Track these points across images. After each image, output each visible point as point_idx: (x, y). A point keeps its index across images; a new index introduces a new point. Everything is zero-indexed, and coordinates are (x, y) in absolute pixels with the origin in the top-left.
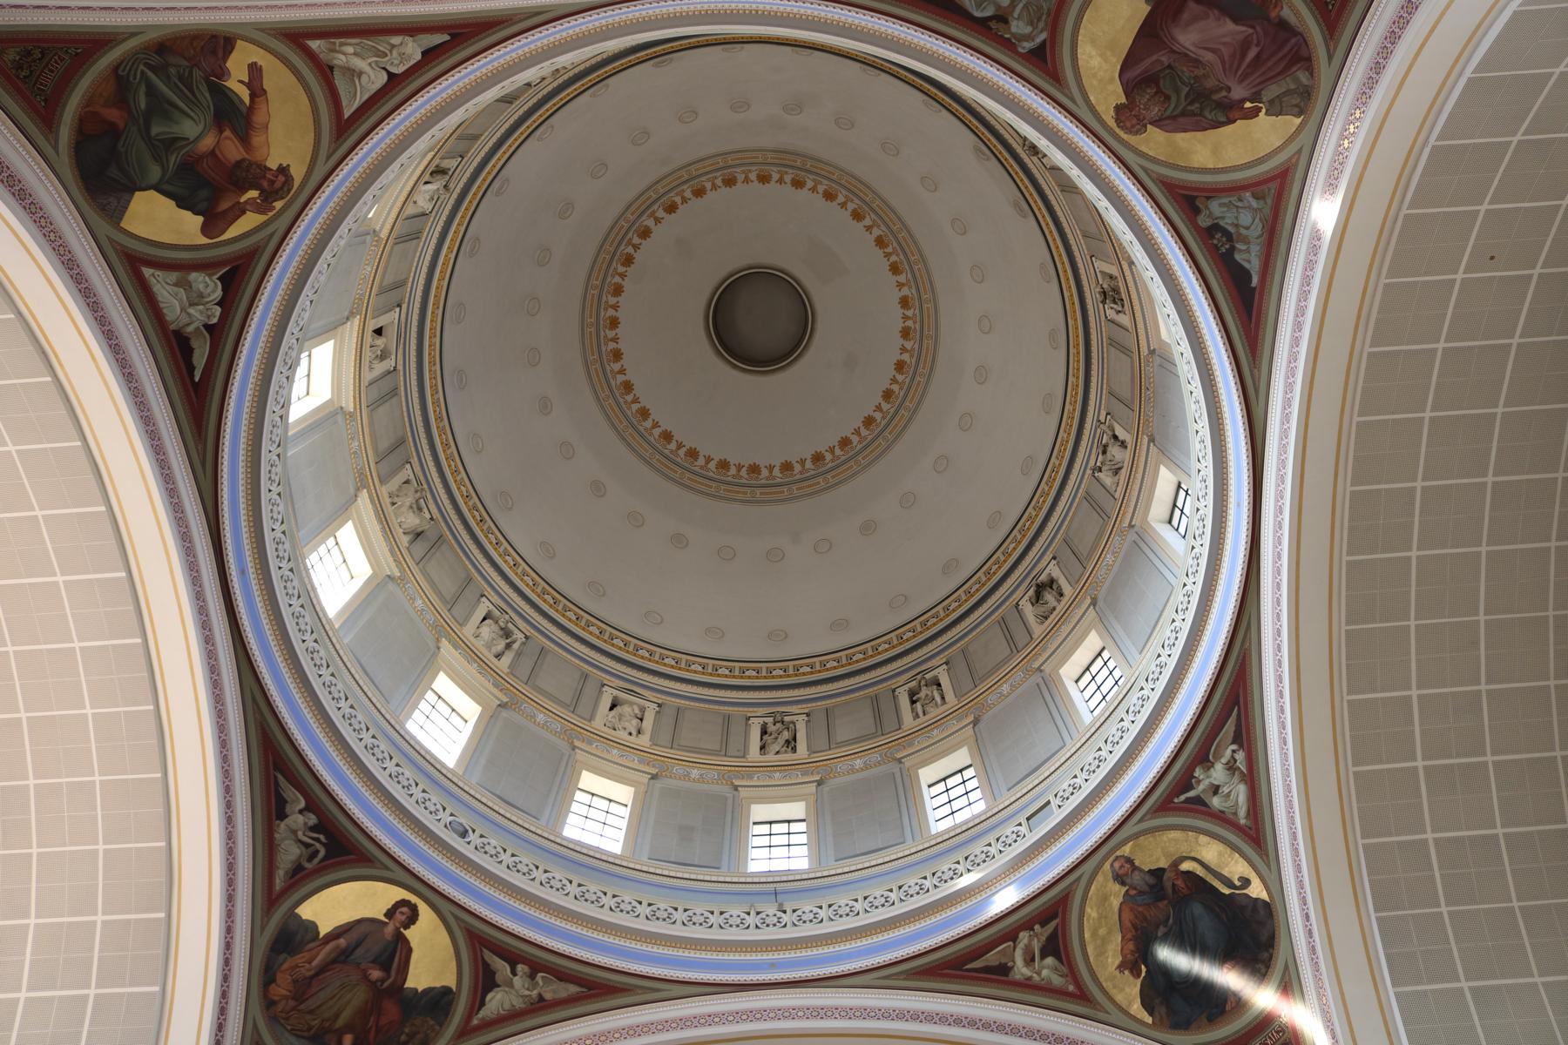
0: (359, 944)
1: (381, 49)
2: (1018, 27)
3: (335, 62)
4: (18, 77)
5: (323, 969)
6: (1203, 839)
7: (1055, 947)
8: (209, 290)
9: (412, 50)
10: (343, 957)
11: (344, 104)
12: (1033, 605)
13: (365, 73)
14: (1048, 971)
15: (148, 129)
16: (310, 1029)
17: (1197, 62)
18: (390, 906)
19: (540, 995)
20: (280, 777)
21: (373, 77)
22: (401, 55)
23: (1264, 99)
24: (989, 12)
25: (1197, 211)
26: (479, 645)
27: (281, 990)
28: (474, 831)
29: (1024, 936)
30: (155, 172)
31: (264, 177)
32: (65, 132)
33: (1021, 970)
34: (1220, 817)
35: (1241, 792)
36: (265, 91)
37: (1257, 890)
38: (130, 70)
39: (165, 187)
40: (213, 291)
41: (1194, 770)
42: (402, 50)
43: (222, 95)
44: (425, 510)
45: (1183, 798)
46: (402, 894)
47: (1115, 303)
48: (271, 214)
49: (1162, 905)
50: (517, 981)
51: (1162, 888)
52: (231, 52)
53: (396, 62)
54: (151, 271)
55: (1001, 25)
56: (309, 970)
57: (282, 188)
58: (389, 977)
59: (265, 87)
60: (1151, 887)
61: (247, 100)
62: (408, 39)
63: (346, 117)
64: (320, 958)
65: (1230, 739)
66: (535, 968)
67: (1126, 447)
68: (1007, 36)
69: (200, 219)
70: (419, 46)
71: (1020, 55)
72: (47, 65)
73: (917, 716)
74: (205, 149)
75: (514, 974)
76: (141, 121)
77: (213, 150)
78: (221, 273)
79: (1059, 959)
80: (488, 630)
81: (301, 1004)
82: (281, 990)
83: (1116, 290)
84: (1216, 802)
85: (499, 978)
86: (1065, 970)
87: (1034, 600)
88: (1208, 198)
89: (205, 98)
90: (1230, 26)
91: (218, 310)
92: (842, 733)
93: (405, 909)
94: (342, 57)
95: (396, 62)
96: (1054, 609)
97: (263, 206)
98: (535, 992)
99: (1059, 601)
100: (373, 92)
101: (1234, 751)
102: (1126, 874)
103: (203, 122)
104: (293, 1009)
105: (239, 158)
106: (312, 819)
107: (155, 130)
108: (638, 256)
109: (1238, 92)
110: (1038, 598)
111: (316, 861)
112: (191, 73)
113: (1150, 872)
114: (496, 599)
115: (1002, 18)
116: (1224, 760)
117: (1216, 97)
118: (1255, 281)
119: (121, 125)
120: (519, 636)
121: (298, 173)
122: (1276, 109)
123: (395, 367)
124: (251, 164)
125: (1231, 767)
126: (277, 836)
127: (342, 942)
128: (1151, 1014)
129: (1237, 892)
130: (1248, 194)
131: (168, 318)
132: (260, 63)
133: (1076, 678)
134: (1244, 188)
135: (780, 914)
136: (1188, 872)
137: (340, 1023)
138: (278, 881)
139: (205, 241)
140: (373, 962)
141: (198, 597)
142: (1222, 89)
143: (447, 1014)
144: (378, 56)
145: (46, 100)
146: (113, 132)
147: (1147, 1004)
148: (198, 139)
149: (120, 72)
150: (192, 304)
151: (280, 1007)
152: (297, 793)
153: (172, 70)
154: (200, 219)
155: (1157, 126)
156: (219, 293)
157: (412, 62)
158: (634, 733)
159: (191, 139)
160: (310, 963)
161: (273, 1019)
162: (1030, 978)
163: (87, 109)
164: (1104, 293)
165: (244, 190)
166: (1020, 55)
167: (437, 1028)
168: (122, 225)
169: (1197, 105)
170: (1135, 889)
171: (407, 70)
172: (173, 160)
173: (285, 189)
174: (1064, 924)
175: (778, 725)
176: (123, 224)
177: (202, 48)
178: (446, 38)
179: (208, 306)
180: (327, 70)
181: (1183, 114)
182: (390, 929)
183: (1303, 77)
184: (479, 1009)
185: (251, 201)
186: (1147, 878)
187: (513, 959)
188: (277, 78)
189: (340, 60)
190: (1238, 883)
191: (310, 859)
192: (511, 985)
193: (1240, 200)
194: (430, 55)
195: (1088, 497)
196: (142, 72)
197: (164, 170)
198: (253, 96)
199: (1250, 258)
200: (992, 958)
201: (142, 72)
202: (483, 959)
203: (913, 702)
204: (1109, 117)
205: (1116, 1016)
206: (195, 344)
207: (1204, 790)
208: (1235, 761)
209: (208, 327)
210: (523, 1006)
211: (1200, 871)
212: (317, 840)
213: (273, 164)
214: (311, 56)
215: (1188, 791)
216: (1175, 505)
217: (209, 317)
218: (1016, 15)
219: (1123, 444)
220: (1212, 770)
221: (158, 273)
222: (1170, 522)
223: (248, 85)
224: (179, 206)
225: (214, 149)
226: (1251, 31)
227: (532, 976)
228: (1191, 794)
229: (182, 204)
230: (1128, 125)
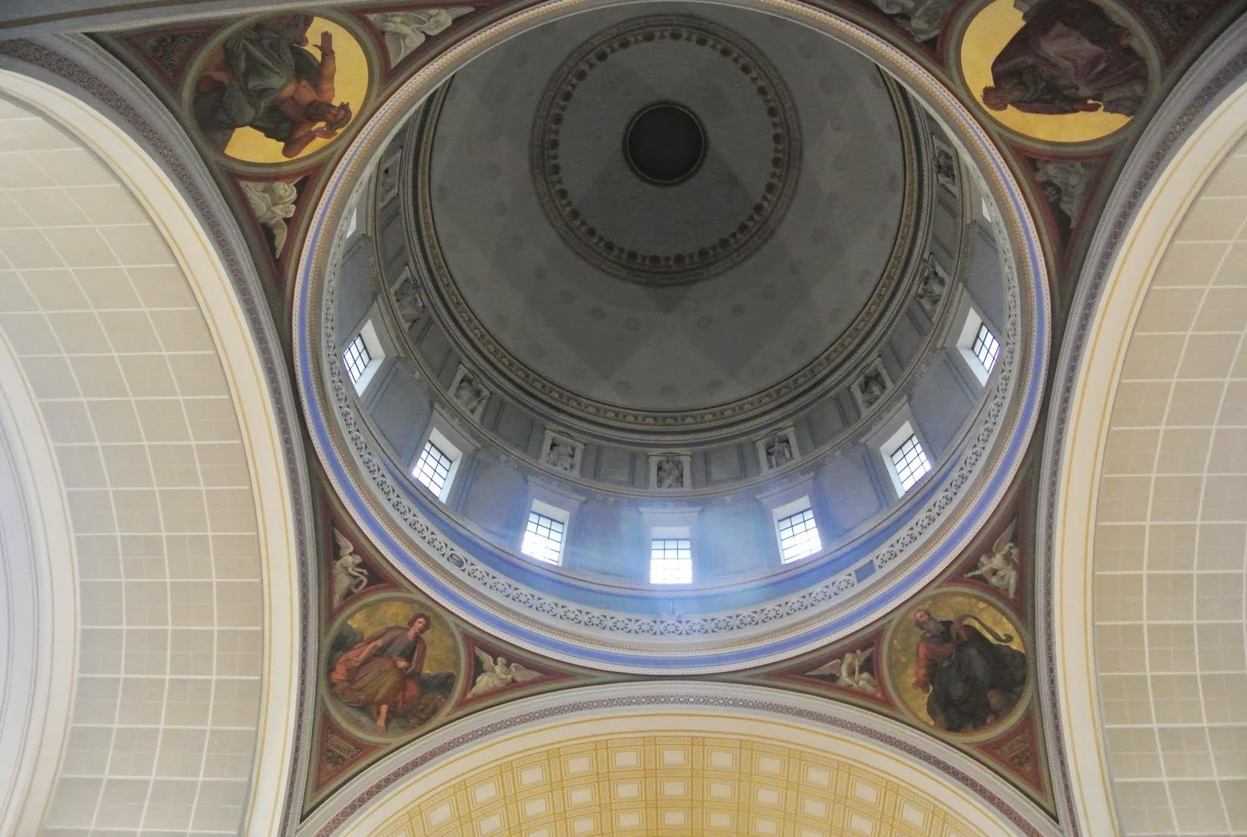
0: (390, 644)
1: (422, 18)
2: (917, 23)
3: (389, 29)
5: (366, 662)
6: (982, 605)
7: (869, 666)
8: (287, 194)
10: (380, 653)
11: (392, 58)
12: (862, 392)
14: (863, 681)
15: (246, 84)
16: (359, 701)
17: (1055, 66)
18: (411, 617)
19: (514, 681)
20: (336, 531)
22: (437, 22)
23: (1105, 99)
24: (896, 11)
25: (1036, 170)
26: (458, 402)
27: (339, 674)
28: (466, 561)
29: (849, 657)
30: (250, 113)
31: (330, 113)
32: (187, 92)
33: (845, 679)
34: (995, 591)
35: (1011, 577)
36: (332, 52)
37: (1016, 645)
39: (257, 123)
40: (290, 195)
41: (980, 557)
42: (438, 18)
44: (419, 300)
45: (970, 575)
46: (418, 610)
47: (948, 176)
48: (333, 138)
49: (949, 646)
50: (498, 668)
51: (949, 635)
54: (246, 183)
55: (904, 21)
56: (358, 662)
57: (344, 117)
58: (411, 666)
60: (943, 633)
61: (319, 58)
62: (443, 12)
64: (365, 653)
65: (1010, 536)
66: (510, 660)
67: (944, 285)
68: (907, 29)
69: (282, 144)
71: (916, 43)
73: (771, 467)
75: (496, 663)
77: (292, 97)
78: (296, 181)
79: (871, 672)
80: (466, 394)
81: (352, 684)
82: (339, 674)
83: (950, 168)
84: (994, 581)
85: (485, 666)
86: (876, 682)
87: (863, 388)
88: (1047, 162)
90: (1087, 45)
91: (293, 208)
92: (717, 473)
93: (421, 620)
96: (878, 398)
97: (326, 135)
98: (510, 676)
99: (882, 392)
101: (1011, 548)
102: (925, 622)
104: (348, 688)
105: (311, 99)
106: (358, 559)
107: (251, 85)
108: (576, 93)
109: (1084, 91)
110: (865, 387)
111: (361, 588)
113: (942, 622)
114: (469, 365)
115: (906, 16)
116: (1003, 553)
117: (1066, 92)
118: (1073, 225)
119: (227, 82)
120: (485, 393)
121: (355, 108)
122: (1112, 108)
123: (398, 194)
125: (1007, 558)
126: (334, 571)
127: (379, 643)
128: (934, 718)
129: (1003, 644)
130: (1078, 164)
131: (257, 216)
132: (330, 32)
133: (891, 453)
134: (1075, 158)
135: (678, 624)
136: (969, 628)
137: (379, 697)
138: (335, 602)
139: (285, 159)
140: (399, 656)
141: (280, 411)
142: (1072, 87)
143: (450, 691)
144: (419, 23)
146: (220, 87)
147: (931, 712)
148: (282, 89)
150: (274, 205)
151: (340, 686)
152: (349, 543)
153: (266, 42)
154: (282, 144)
155: (1018, 108)
156: (294, 196)
157: (445, 27)
158: (568, 467)
160: (358, 657)
161: (334, 696)
162: (850, 686)
164: (939, 167)
165: (314, 121)
166: (916, 43)
167: (444, 700)
168: (226, 152)
169: (1050, 96)
170: (929, 632)
171: (441, 32)
173: (345, 120)
174: (878, 652)
175: (671, 464)
176: (228, 152)
179: (287, 205)
181: (1038, 100)
182: (411, 634)
183: (1139, 89)
184: (472, 687)
185: (320, 129)
186: (940, 625)
187: (495, 654)
189: (390, 27)
190: (1004, 638)
191: (357, 586)
192: (493, 671)
193: (1072, 167)
194: (458, 22)
195: (909, 314)
198: (324, 56)
199: (1072, 208)
200: (825, 669)
201: (244, 45)
202: (474, 653)
203: (769, 454)
204: (978, 96)
205: (908, 717)
206: (276, 232)
207: (986, 571)
208: (1011, 554)
209: (287, 220)
210: (501, 686)
211: (977, 626)
212: (362, 573)
213: (336, 102)
214: (369, 25)
215: (975, 570)
216: (978, 337)
217: (286, 212)
218: (917, 15)
219: (942, 282)
220: (993, 558)
221: (249, 184)
222: (973, 348)
224: (268, 136)
226: (1101, 50)
227: (508, 665)
228: (977, 573)
229: (269, 134)
230: (993, 102)
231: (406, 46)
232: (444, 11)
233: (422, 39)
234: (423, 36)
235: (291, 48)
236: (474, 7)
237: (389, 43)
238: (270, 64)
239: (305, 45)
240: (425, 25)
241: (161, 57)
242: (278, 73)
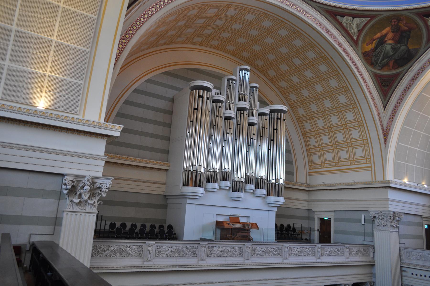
9: (345, 20)
13: (356, 23)
15: (393, 55)
21: (356, 22)
39: (406, 43)
52: (366, 52)
53: (350, 20)
62: (343, 23)
63: (369, 19)
70: (343, 19)
74: (392, 41)
76: (391, 57)
77: (392, 39)
89: (379, 49)
94: (355, 31)
95: (350, 20)
100: (360, 18)
103: (386, 46)
105: (391, 33)
107: (392, 54)
112: (375, 55)
119: (393, 61)
124: (392, 30)
148: (390, 44)
149: (380, 68)
153: (376, 59)
159: (391, 45)
163: (392, 69)
172: (397, 46)
177: (368, 57)
178: (337, 17)
180: (360, 31)
189: (356, 31)
194: (343, 16)
196: (379, 64)
197: (400, 47)
201: (379, 64)
223: (372, 43)
225: (392, 39)
231: (360, 21)
232: (342, 22)
233: (356, 19)
235: (375, 51)
237: (361, 26)
238: (383, 53)
241: (389, 83)
242: (385, 49)
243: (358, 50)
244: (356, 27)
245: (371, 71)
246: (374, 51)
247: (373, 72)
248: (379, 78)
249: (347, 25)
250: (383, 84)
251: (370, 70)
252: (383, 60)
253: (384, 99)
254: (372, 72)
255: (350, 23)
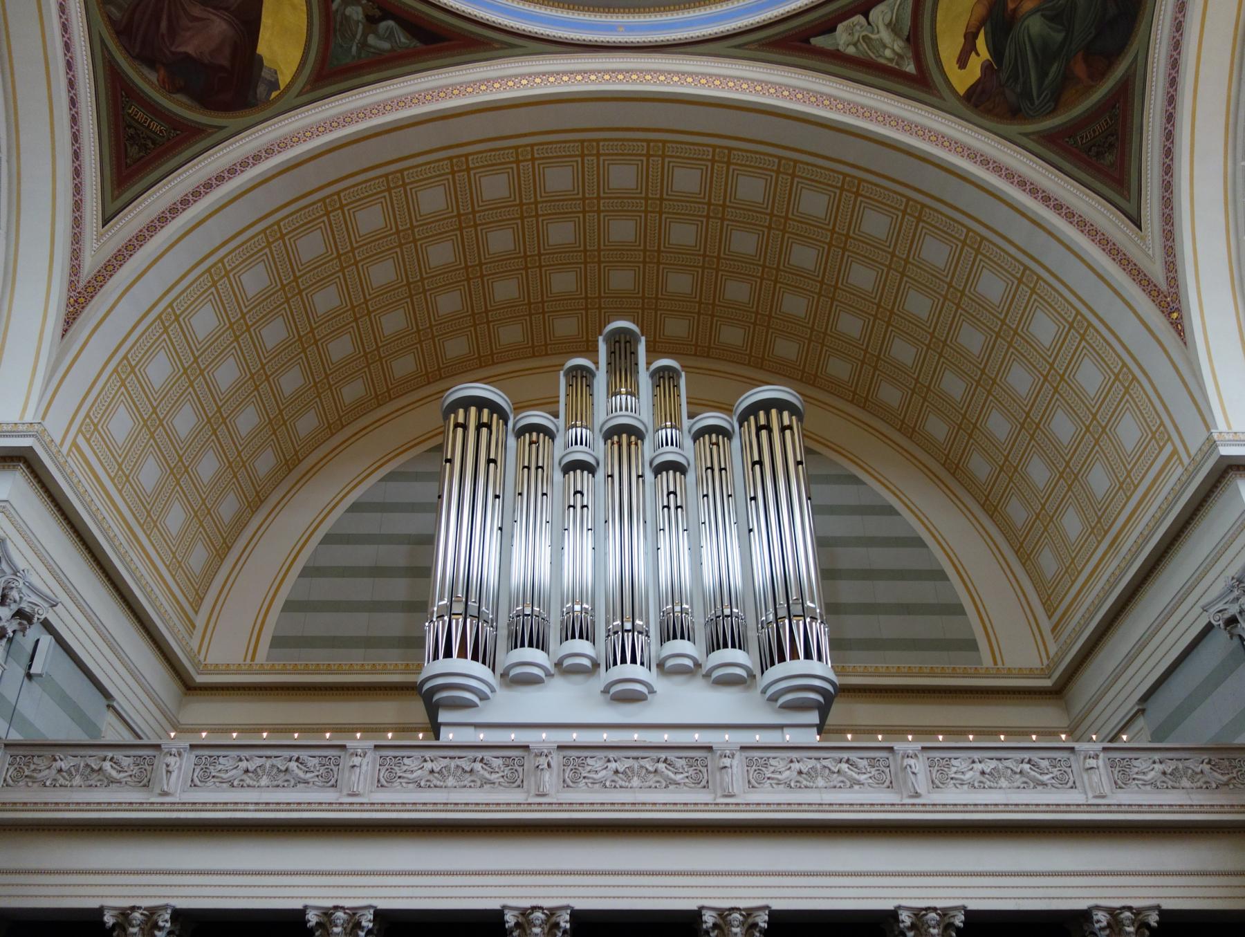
3: (901, 44)
4: (1117, 139)
21: (881, 18)
38: (1046, 104)
43: (996, 50)
52: (972, 86)
59: (963, 40)
70: (836, 39)
72: (1094, 138)
94: (896, 47)
112: (1008, 80)
132: (957, 66)
144: (870, 39)
145: (1114, 107)
153: (1018, 90)
157: (845, 23)
180: (912, 39)
188: (949, 48)
189: (898, 45)
194: (828, 27)
198: (975, 36)
201: (1039, 96)
232: (840, 48)
233: (875, 14)
234: (871, 18)
236: (810, 43)
239: (988, 60)
240: (864, 33)
243: (941, 97)
244: (893, 35)
245: (1026, 135)
246: (996, 68)
247: (1033, 133)
248: (1067, 140)
249: (860, 47)
250: (1090, 150)
251: (1020, 134)
252: (1046, 74)
253: (1125, 198)
254: (1031, 137)
255: (866, 35)
